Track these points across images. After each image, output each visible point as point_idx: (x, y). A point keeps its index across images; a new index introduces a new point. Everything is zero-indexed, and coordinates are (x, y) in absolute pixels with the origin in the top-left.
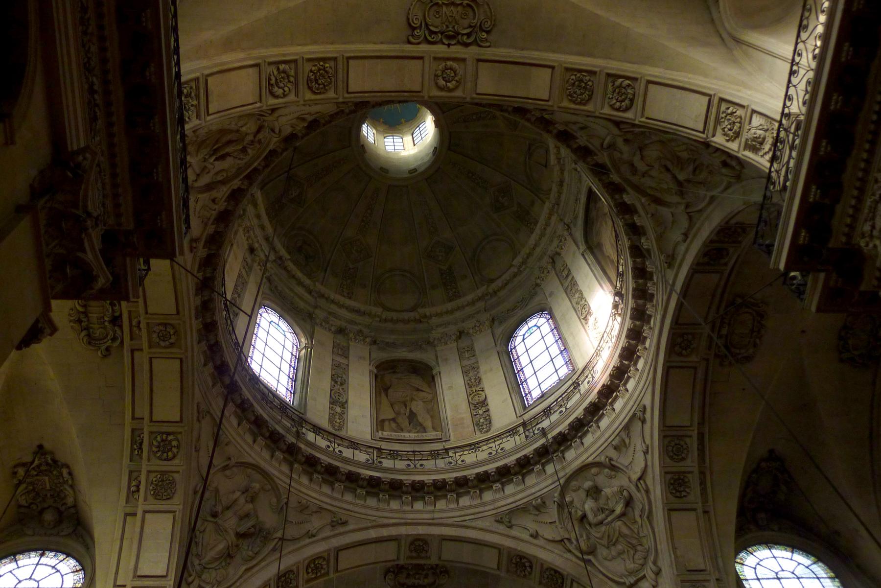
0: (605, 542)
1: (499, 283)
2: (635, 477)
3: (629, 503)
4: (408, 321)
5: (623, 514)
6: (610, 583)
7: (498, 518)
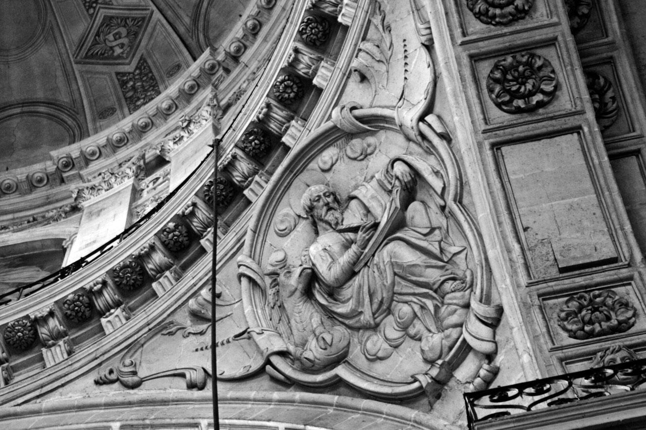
0: (367, 317)
1: (237, 31)
2: (408, 116)
3: (412, 188)
4: (32, 184)
5: (399, 223)
6: (385, 407)
7: (103, 372)
